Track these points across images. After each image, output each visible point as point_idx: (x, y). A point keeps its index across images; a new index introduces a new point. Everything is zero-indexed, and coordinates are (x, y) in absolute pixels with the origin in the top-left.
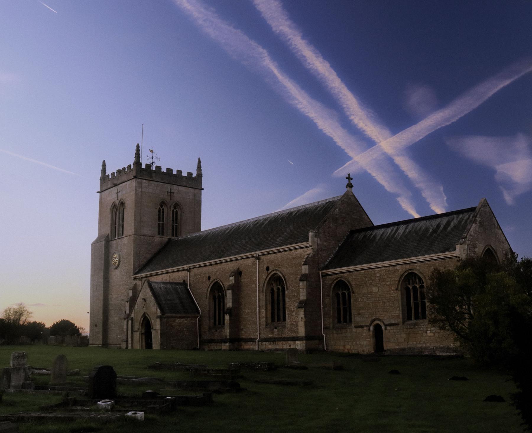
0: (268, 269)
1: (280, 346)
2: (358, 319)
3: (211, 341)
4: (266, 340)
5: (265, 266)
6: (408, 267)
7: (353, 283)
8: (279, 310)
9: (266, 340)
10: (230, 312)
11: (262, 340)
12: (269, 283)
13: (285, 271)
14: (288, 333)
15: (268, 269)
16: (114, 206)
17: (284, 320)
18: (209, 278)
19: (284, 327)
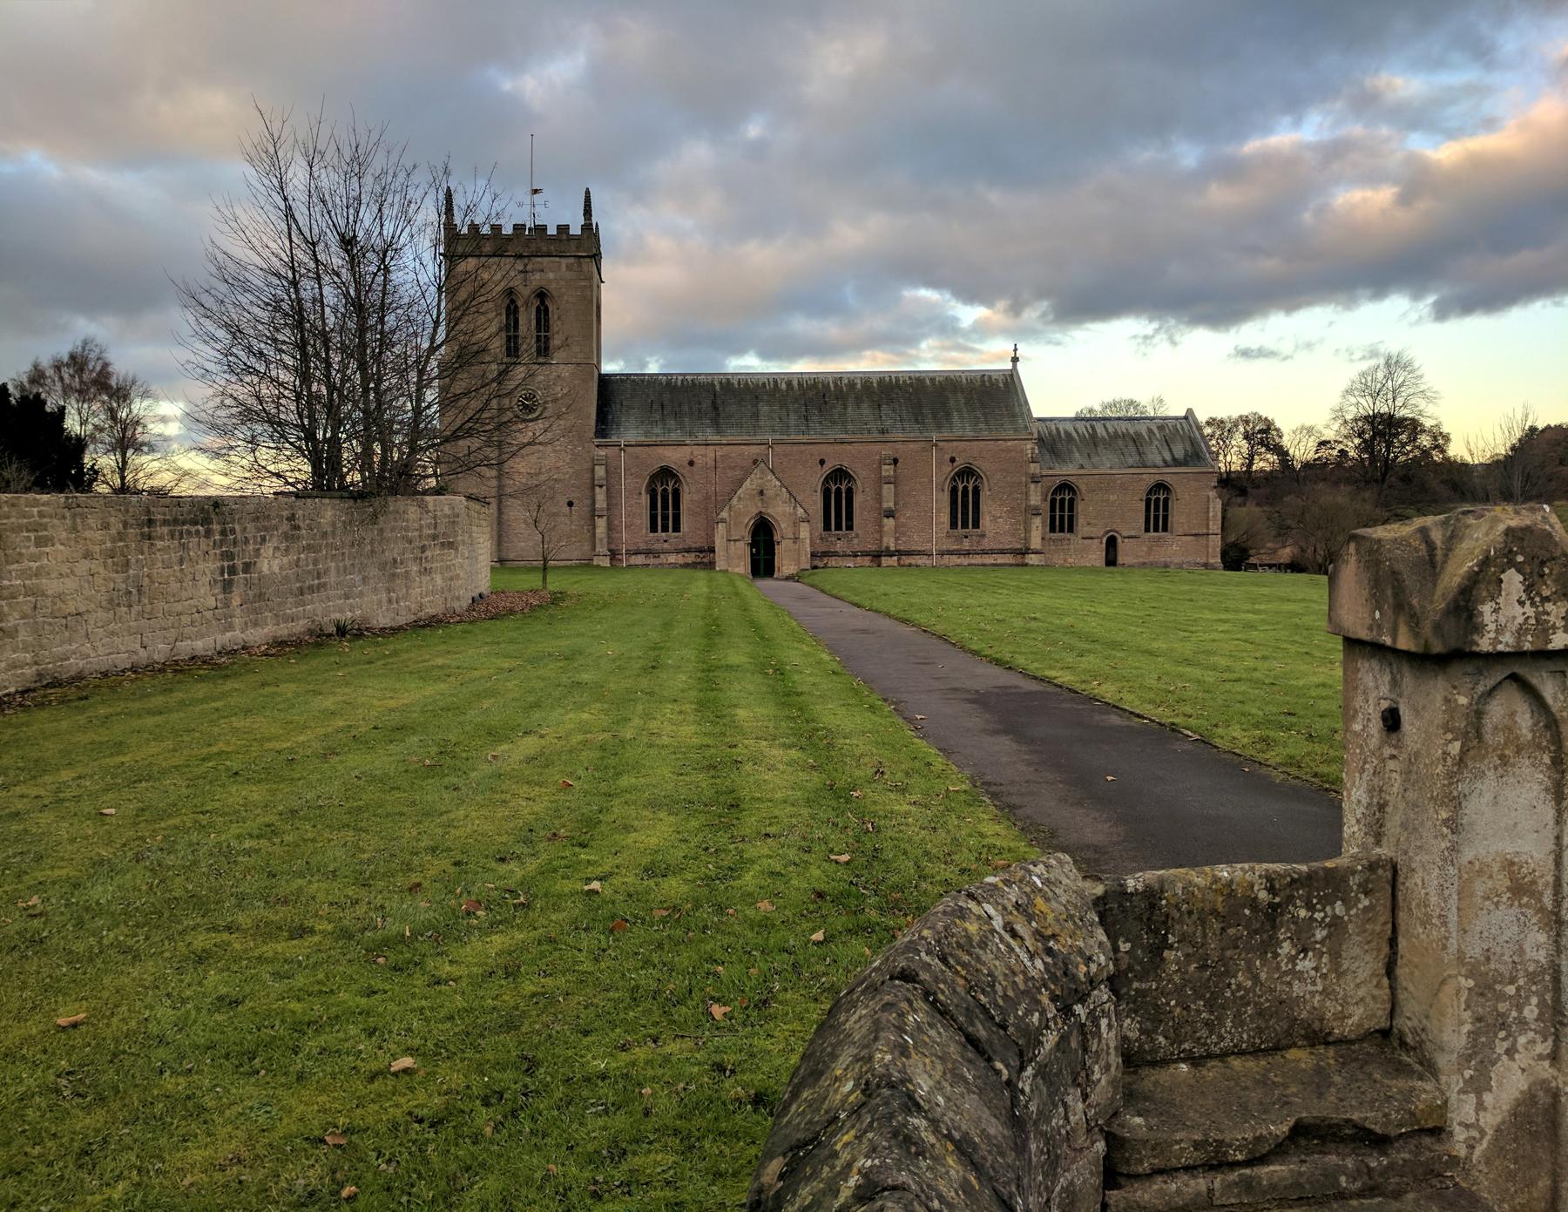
0: (953, 460)
1: (977, 560)
2: (1086, 529)
3: (826, 554)
4: (951, 553)
5: (948, 457)
6: (1158, 477)
7: (1083, 488)
8: (965, 514)
9: (951, 553)
10: (890, 514)
11: (942, 554)
12: (953, 479)
13: (982, 466)
14: (986, 544)
15: (953, 460)
16: (510, 292)
17: (976, 525)
18: (822, 462)
19: (983, 536)
